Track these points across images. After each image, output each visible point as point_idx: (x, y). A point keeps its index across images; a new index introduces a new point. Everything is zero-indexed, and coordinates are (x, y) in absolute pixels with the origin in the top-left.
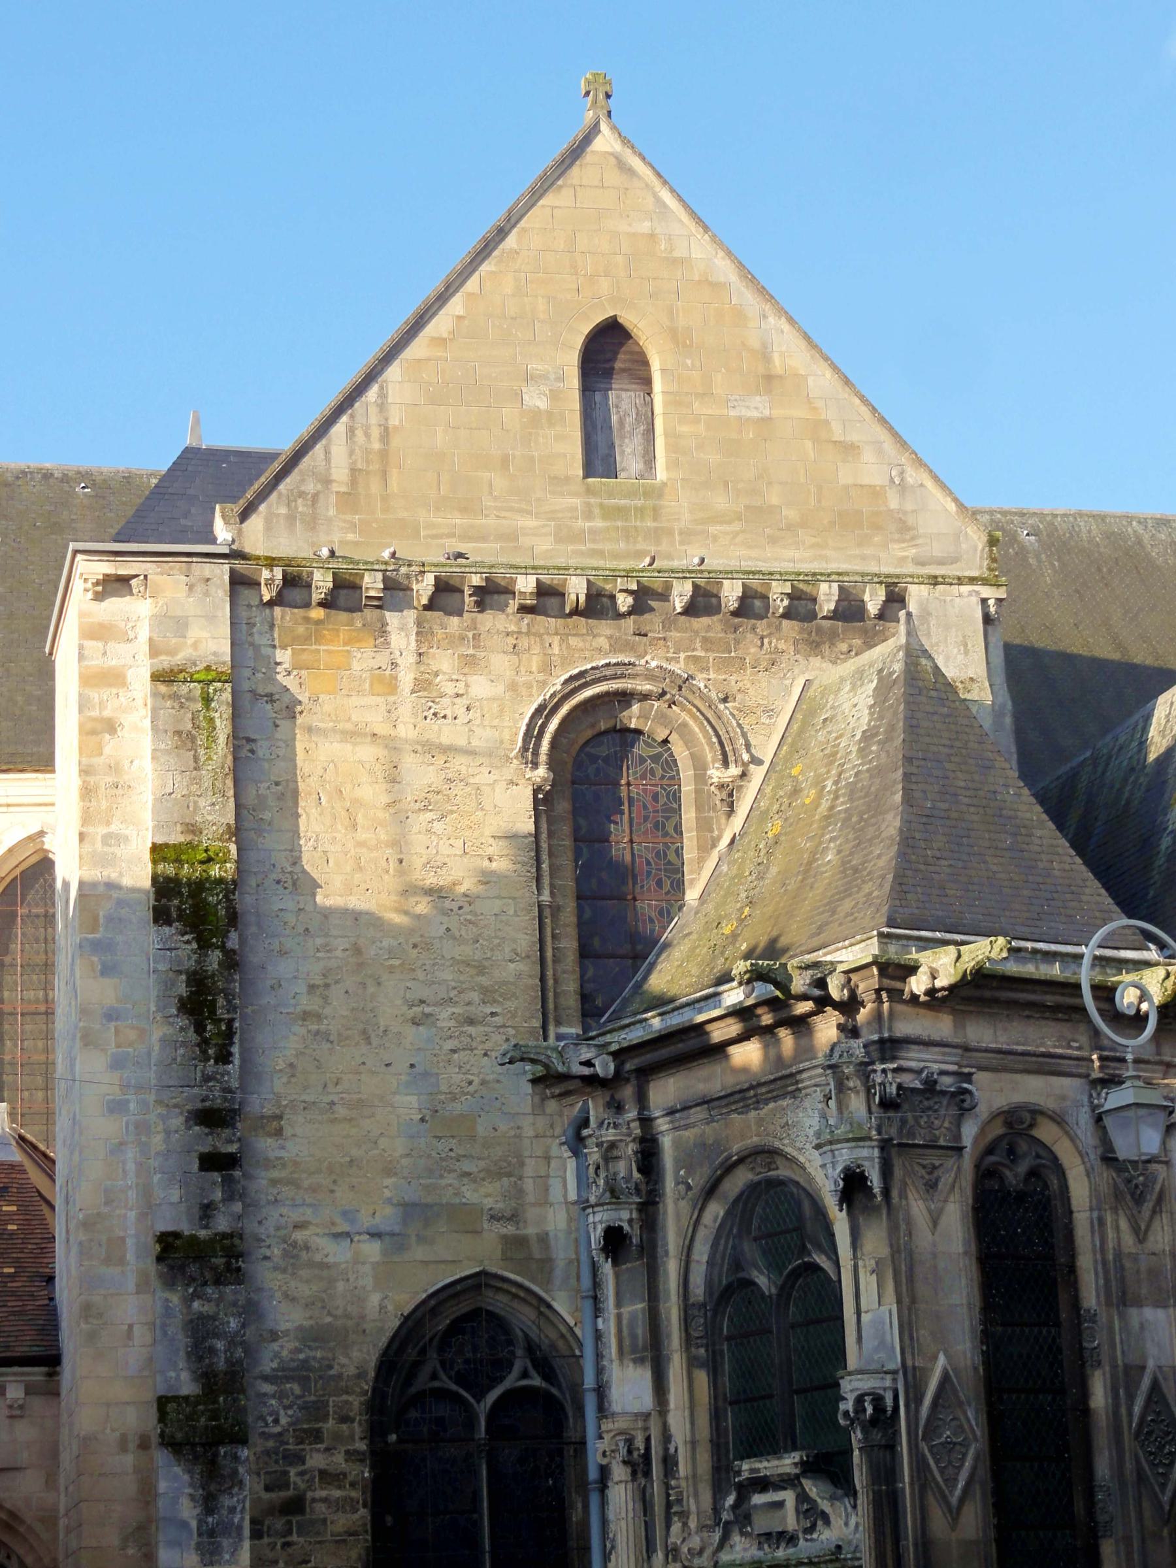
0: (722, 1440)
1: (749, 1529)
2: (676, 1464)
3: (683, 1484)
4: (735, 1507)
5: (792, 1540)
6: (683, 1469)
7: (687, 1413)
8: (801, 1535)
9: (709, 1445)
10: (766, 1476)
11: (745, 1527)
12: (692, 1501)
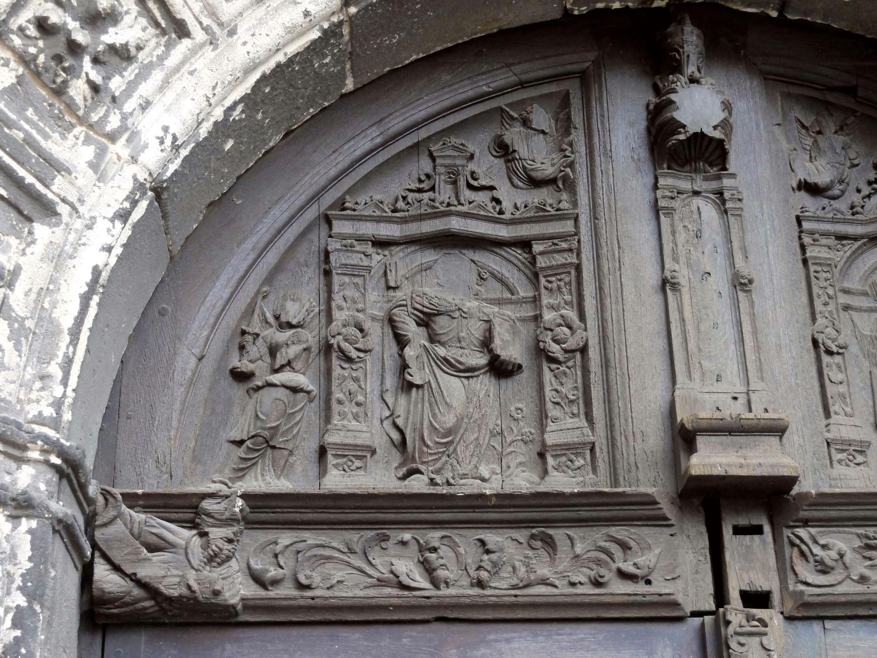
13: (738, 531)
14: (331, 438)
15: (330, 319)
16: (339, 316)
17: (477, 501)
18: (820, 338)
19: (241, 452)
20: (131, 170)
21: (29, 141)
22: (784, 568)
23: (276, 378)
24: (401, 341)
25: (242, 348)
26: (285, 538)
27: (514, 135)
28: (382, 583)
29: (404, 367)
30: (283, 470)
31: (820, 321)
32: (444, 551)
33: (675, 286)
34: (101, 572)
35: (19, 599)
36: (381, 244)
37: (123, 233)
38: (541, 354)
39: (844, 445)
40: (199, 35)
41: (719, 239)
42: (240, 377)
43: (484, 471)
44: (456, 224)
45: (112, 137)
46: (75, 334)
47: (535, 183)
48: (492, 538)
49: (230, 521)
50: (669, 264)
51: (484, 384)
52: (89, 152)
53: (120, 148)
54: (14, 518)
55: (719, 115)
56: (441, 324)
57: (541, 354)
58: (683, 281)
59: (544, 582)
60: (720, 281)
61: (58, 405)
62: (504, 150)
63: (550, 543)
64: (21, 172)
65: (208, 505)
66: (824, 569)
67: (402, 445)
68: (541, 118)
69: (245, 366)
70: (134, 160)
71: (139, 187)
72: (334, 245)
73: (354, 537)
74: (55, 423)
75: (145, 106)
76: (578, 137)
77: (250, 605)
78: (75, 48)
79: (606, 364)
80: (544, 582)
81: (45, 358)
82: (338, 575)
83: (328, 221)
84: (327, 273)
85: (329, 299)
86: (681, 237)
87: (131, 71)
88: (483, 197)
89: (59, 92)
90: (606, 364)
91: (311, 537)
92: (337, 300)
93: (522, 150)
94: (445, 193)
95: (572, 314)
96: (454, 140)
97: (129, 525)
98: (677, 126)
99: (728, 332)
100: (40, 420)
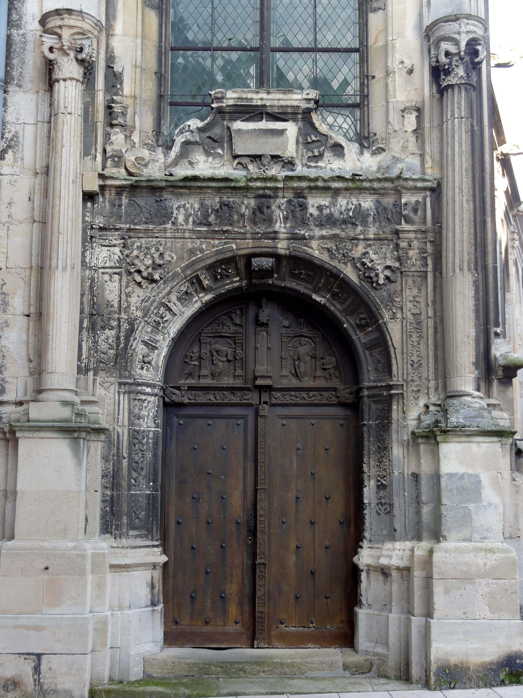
0: (166, 76)
1: (220, 151)
2: (121, 83)
3: (129, 102)
4: (200, 130)
5: (290, 163)
6: (127, 88)
7: (139, 40)
8: (298, 162)
9: (153, 77)
10: (264, 106)
11: (214, 148)
12: (137, 119)
13: (264, 391)
14: (201, 374)
15: (201, 352)
16: (202, 351)
17: (222, 388)
18: (283, 357)
19: (186, 376)
20: (169, 339)
21: (154, 339)
22: (270, 398)
23: (192, 363)
24: (213, 356)
25: (186, 357)
26: (193, 392)
27: (233, 315)
28: (208, 400)
29: (213, 361)
30: (193, 378)
31: (283, 353)
32: (218, 394)
33: (258, 349)
34: (166, 399)
35: (157, 409)
36: (209, 337)
37: (167, 348)
38: (235, 358)
39: (283, 376)
40: (179, 315)
41: (266, 339)
42: (186, 362)
43: (225, 379)
44: (222, 334)
45: (166, 334)
46: (161, 367)
47: (236, 325)
48: (225, 393)
49: (185, 390)
50: (257, 345)
51: (226, 364)
52: (162, 337)
53: (167, 336)
54: (155, 397)
55: (267, 318)
56: (220, 353)
57: (235, 358)
58: (259, 348)
59: (233, 400)
60: (265, 348)
61: (159, 378)
62: (232, 319)
63: (234, 394)
64: (153, 344)
65: (182, 388)
66: (276, 398)
67: (212, 374)
68: (238, 312)
69: (187, 360)
70: (169, 337)
71: (170, 341)
72: (202, 338)
73: (204, 392)
74: (159, 381)
75: (170, 328)
76: (244, 316)
77: (188, 403)
78: (160, 323)
79: (246, 361)
80: (233, 400)
81: (157, 371)
82: (201, 398)
83: (200, 333)
84: (200, 343)
85: (201, 348)
86: (260, 339)
87: (168, 323)
88: (227, 328)
89: (158, 329)
90: (246, 361)
91: (197, 392)
92: (202, 348)
93: (234, 319)
94: (221, 327)
95: (240, 351)
96: (223, 317)
97: (170, 391)
98: (259, 320)
99: (266, 357)
100: (157, 381)
